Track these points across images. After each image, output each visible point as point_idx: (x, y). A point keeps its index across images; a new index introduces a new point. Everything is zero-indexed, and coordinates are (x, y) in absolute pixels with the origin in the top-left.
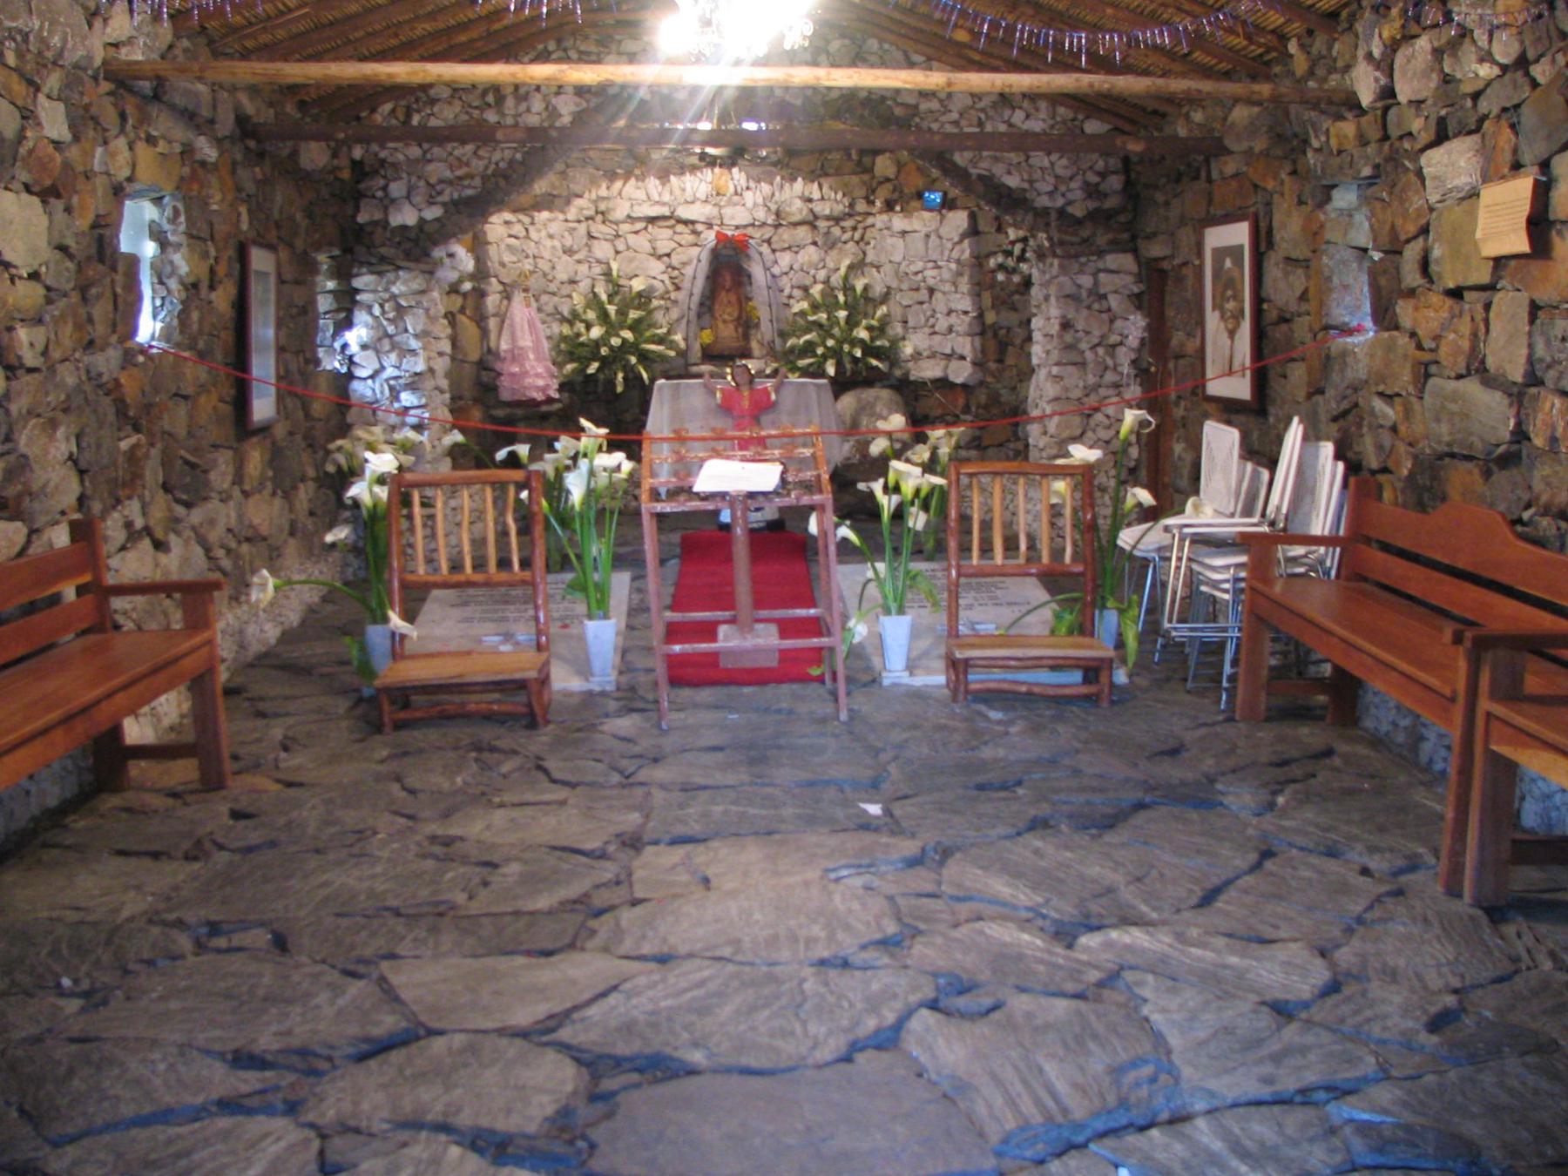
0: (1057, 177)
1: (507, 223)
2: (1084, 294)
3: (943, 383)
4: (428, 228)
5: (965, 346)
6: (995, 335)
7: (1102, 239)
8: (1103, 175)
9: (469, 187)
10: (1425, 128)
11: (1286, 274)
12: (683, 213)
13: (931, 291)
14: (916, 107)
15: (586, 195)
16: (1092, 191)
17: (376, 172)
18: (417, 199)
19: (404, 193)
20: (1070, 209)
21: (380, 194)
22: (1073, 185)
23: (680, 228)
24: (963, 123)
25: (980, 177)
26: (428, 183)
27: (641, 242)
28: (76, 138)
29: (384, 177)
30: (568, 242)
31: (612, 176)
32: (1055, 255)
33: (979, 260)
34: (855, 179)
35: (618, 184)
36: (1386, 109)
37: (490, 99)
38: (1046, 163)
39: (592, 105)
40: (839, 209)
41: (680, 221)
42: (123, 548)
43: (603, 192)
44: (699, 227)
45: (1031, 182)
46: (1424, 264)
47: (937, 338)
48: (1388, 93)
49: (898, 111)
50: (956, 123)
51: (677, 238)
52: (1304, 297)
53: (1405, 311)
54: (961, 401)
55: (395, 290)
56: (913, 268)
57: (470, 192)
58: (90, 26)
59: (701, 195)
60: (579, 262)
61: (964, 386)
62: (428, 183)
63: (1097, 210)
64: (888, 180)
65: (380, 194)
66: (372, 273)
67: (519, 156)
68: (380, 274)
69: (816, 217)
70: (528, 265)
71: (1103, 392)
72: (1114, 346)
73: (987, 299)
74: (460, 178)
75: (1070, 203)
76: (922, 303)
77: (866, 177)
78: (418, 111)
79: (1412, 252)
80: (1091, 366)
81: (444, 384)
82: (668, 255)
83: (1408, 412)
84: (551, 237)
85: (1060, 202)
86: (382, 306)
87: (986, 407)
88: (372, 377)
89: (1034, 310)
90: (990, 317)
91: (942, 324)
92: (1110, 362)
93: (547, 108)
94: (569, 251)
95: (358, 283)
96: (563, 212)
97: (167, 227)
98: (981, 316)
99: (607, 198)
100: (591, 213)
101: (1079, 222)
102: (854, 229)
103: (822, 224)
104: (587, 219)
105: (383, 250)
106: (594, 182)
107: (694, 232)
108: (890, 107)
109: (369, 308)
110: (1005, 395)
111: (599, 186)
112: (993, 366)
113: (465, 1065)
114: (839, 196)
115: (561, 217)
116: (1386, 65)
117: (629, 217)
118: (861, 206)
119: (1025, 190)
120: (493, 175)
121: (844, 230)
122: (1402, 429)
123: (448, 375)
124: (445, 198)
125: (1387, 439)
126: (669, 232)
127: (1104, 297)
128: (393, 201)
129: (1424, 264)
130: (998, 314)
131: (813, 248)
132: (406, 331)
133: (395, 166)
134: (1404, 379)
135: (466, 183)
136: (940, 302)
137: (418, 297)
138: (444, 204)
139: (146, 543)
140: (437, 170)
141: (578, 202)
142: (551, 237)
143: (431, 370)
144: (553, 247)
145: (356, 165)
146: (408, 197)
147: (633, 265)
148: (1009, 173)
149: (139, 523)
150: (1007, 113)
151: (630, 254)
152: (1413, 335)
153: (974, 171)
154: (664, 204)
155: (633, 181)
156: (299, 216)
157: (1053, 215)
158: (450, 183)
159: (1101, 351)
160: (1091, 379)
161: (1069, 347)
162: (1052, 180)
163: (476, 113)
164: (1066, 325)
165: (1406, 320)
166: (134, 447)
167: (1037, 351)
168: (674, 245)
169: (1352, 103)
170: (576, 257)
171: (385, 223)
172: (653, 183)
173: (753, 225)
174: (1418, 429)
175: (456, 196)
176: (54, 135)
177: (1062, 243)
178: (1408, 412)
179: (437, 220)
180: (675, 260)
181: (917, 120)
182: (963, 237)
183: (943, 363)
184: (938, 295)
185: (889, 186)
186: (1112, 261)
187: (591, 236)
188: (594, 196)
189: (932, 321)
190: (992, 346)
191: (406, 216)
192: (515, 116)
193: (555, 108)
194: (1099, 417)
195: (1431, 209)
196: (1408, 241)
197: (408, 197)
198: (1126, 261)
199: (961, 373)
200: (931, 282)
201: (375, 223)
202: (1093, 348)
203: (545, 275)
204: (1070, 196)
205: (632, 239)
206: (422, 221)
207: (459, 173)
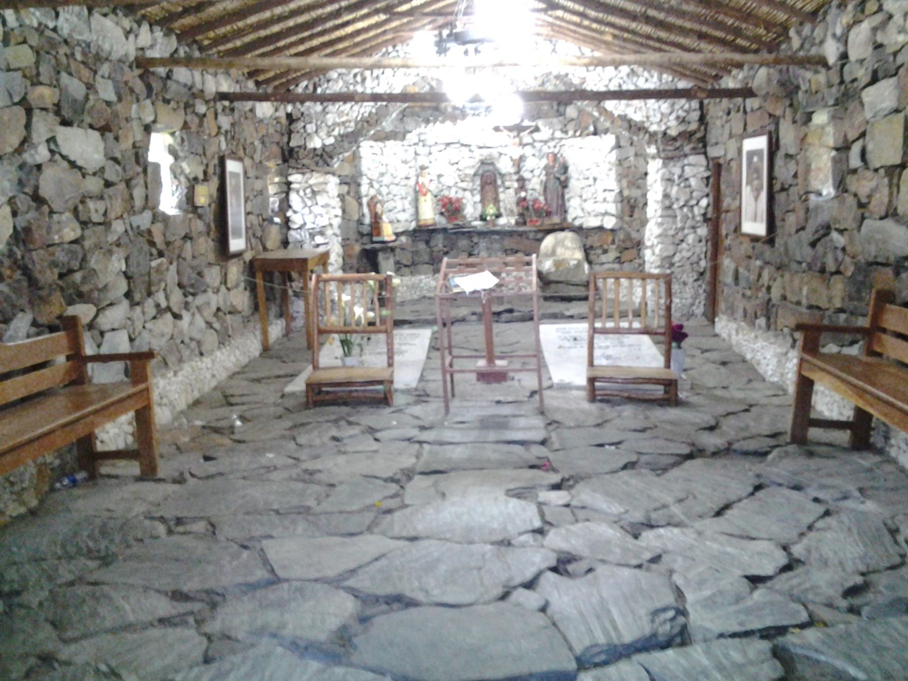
0: (662, 114)
2: (676, 177)
3: (601, 228)
4: (327, 149)
5: (612, 208)
6: (629, 202)
7: (687, 149)
8: (687, 112)
10: (865, 75)
11: (786, 164)
13: (595, 179)
16: (682, 121)
25: (619, 116)
28: (120, 99)
33: (620, 162)
34: (555, 120)
36: (843, 66)
37: (359, 79)
40: (545, 138)
42: (154, 318)
46: (863, 154)
48: (844, 56)
52: (795, 176)
53: (852, 183)
54: (610, 239)
55: (312, 182)
57: (350, 130)
58: (127, 38)
61: (612, 230)
63: (685, 132)
64: (572, 120)
67: (374, 111)
68: (303, 174)
70: (383, 169)
71: (686, 231)
72: (692, 207)
73: (625, 183)
77: (561, 118)
79: (856, 149)
80: (679, 218)
81: (338, 232)
83: (851, 240)
85: (663, 128)
87: (624, 241)
90: (626, 193)
92: (690, 215)
94: (405, 162)
95: (291, 179)
97: (178, 148)
98: (621, 192)
101: (674, 139)
103: (538, 145)
105: (305, 161)
106: (418, 125)
109: (298, 192)
110: (634, 235)
112: (627, 219)
113: (294, 599)
116: (844, 39)
118: (558, 134)
122: (848, 248)
123: (339, 227)
124: (336, 133)
125: (840, 255)
127: (687, 179)
129: (863, 154)
134: (850, 223)
136: (600, 186)
138: (335, 137)
139: (169, 316)
141: (408, 136)
143: (331, 225)
145: (289, 116)
149: (164, 304)
152: (855, 195)
156: (257, 143)
157: (660, 136)
159: (685, 209)
160: (679, 225)
161: (669, 207)
164: (666, 196)
165: (852, 188)
166: (160, 265)
169: (822, 62)
174: (859, 248)
176: (107, 98)
177: (664, 150)
178: (851, 240)
180: (460, 166)
185: (573, 123)
186: (692, 159)
187: (416, 154)
190: (627, 208)
191: (316, 143)
194: (684, 245)
195: (867, 123)
196: (854, 141)
197: (316, 132)
198: (701, 159)
199: (610, 223)
201: (300, 147)
202: (681, 208)
204: (669, 124)
207: (344, 119)
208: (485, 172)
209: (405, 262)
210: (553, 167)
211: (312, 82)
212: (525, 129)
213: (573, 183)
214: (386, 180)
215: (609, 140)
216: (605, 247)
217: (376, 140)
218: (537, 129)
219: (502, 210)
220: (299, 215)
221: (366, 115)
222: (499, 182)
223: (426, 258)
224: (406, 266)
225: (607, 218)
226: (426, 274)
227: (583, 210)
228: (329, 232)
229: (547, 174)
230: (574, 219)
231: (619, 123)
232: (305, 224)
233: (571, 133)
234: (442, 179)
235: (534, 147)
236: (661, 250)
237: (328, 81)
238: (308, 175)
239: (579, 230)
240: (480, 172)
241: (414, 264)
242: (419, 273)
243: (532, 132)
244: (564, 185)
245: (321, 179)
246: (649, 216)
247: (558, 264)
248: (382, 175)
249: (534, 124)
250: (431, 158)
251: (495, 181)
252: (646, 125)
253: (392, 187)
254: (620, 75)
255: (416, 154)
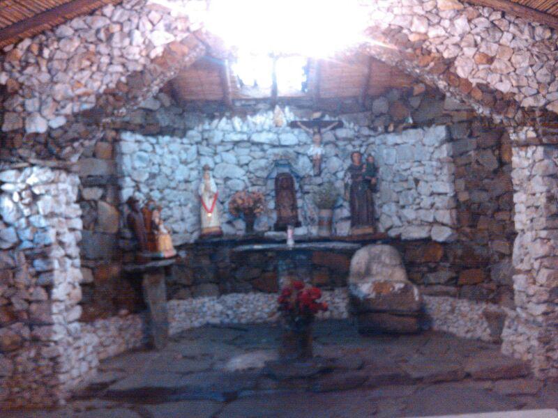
1: (138, 142)
3: (428, 240)
4: (54, 134)
5: (446, 216)
6: (468, 208)
9: (86, 102)
12: (256, 138)
13: (417, 181)
14: (426, 34)
15: (196, 128)
17: (16, 92)
18: (46, 112)
19: (37, 105)
20: (550, 108)
21: (19, 109)
22: (551, 89)
23: (254, 148)
24: (463, 44)
25: (479, 85)
26: (54, 100)
27: (230, 157)
29: (23, 96)
30: (184, 156)
31: (212, 117)
32: (542, 144)
33: (454, 158)
34: (361, 115)
35: (216, 122)
37: (102, 35)
38: (530, 72)
39: (179, 39)
41: (254, 144)
43: (207, 127)
44: (266, 147)
45: (519, 87)
47: (422, 212)
49: (413, 38)
50: (457, 45)
51: (252, 154)
54: (440, 253)
55: (30, 181)
56: (403, 167)
57: (87, 107)
59: (266, 127)
60: (192, 169)
61: (444, 244)
62: (54, 100)
64: (382, 114)
65: (19, 109)
66: (13, 169)
67: (123, 79)
69: (337, 139)
70: (155, 170)
73: (461, 183)
74: (79, 96)
75: (549, 103)
76: (410, 189)
77: (368, 114)
78: (47, 46)
81: (74, 251)
82: (247, 164)
84: (171, 152)
85: (542, 102)
86: (20, 194)
87: (461, 258)
88: (13, 248)
89: (516, 188)
90: (464, 197)
91: (426, 201)
93: (144, 43)
94: (185, 163)
96: (181, 138)
98: (455, 196)
99: (209, 131)
100: (199, 139)
102: (361, 146)
103: (341, 144)
104: (197, 143)
105: (22, 152)
106: (201, 121)
107: (263, 150)
108: (406, 35)
110: (479, 251)
111: (204, 124)
112: (468, 230)
114: (352, 125)
115: (178, 140)
117: (222, 141)
118: (366, 131)
119: (514, 94)
120: (105, 93)
121: (354, 146)
124: (68, 109)
126: (247, 151)
128: (29, 114)
130: (470, 193)
131: (335, 159)
132: (38, 213)
133: (31, 88)
135: (84, 99)
137: (47, 187)
138: (66, 116)
140: (60, 90)
141: (191, 133)
142: (171, 152)
144: (173, 160)
146: (40, 111)
147: (226, 171)
148: (501, 81)
150: (498, 35)
151: (224, 164)
153: (474, 81)
154: (242, 133)
155: (224, 120)
157: (538, 113)
158: (72, 99)
162: (536, 86)
163: (92, 47)
167: (521, 219)
168: (250, 158)
170: (191, 166)
171: (22, 131)
172: (237, 121)
173: (299, 145)
175: (76, 109)
177: (545, 134)
179: (61, 127)
180: (251, 168)
181: (427, 43)
182: (442, 143)
183: (427, 228)
184: (421, 184)
185: (383, 118)
188: (200, 128)
189: (418, 201)
190: (466, 216)
191: (38, 126)
192: (121, 49)
193: (150, 41)
199: (441, 235)
200: (417, 175)
201: (14, 131)
203: (167, 177)
204: (549, 97)
205: (224, 155)
206: (50, 129)
207: (79, 92)
208: (280, 175)
209: (184, 281)
210: (361, 168)
211: (37, 41)
212: (327, 124)
213: (384, 186)
214: (159, 182)
215: (441, 131)
216: (433, 265)
217: (145, 135)
218: (340, 125)
219: (301, 219)
220: (11, 230)
221: (112, 86)
222: (297, 186)
223: (211, 276)
224: (185, 286)
225: (436, 229)
226: (209, 294)
227: (400, 218)
228: (57, 253)
229: (352, 177)
230: (388, 229)
231: (479, 95)
232: (20, 242)
233: (380, 129)
234: (229, 183)
235: (337, 146)
236: (549, 277)
237: (59, 39)
238: (27, 171)
239: (398, 243)
240: (274, 175)
241: (195, 283)
242: (202, 295)
243: (334, 129)
244: (374, 189)
245: (48, 175)
246: (518, 226)
247: (378, 287)
248: (153, 176)
249: (337, 119)
250: (218, 159)
251: (292, 185)
252: (517, 98)
253: (167, 191)
254: (478, 30)
255: (199, 154)
